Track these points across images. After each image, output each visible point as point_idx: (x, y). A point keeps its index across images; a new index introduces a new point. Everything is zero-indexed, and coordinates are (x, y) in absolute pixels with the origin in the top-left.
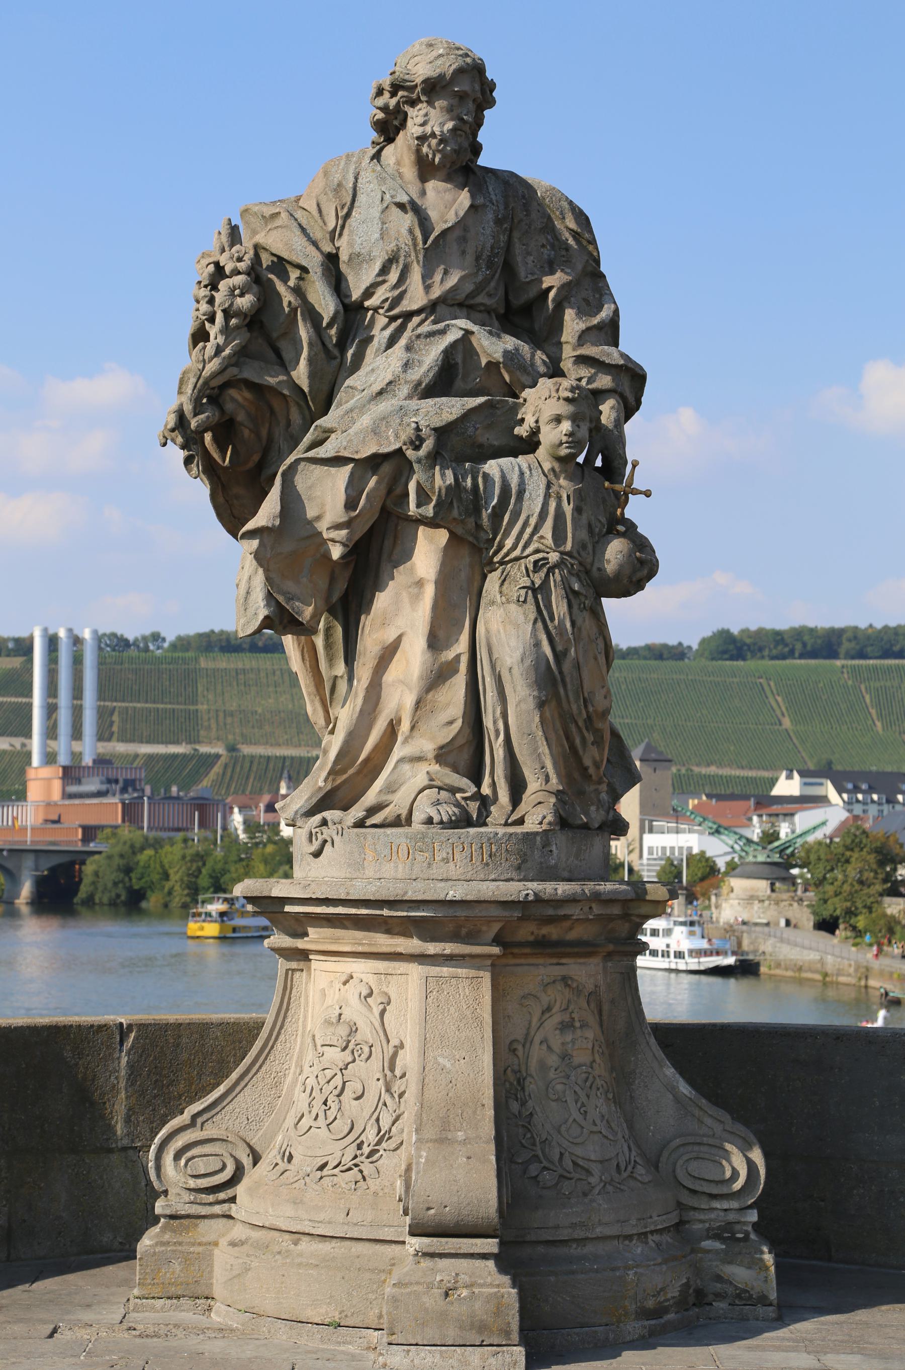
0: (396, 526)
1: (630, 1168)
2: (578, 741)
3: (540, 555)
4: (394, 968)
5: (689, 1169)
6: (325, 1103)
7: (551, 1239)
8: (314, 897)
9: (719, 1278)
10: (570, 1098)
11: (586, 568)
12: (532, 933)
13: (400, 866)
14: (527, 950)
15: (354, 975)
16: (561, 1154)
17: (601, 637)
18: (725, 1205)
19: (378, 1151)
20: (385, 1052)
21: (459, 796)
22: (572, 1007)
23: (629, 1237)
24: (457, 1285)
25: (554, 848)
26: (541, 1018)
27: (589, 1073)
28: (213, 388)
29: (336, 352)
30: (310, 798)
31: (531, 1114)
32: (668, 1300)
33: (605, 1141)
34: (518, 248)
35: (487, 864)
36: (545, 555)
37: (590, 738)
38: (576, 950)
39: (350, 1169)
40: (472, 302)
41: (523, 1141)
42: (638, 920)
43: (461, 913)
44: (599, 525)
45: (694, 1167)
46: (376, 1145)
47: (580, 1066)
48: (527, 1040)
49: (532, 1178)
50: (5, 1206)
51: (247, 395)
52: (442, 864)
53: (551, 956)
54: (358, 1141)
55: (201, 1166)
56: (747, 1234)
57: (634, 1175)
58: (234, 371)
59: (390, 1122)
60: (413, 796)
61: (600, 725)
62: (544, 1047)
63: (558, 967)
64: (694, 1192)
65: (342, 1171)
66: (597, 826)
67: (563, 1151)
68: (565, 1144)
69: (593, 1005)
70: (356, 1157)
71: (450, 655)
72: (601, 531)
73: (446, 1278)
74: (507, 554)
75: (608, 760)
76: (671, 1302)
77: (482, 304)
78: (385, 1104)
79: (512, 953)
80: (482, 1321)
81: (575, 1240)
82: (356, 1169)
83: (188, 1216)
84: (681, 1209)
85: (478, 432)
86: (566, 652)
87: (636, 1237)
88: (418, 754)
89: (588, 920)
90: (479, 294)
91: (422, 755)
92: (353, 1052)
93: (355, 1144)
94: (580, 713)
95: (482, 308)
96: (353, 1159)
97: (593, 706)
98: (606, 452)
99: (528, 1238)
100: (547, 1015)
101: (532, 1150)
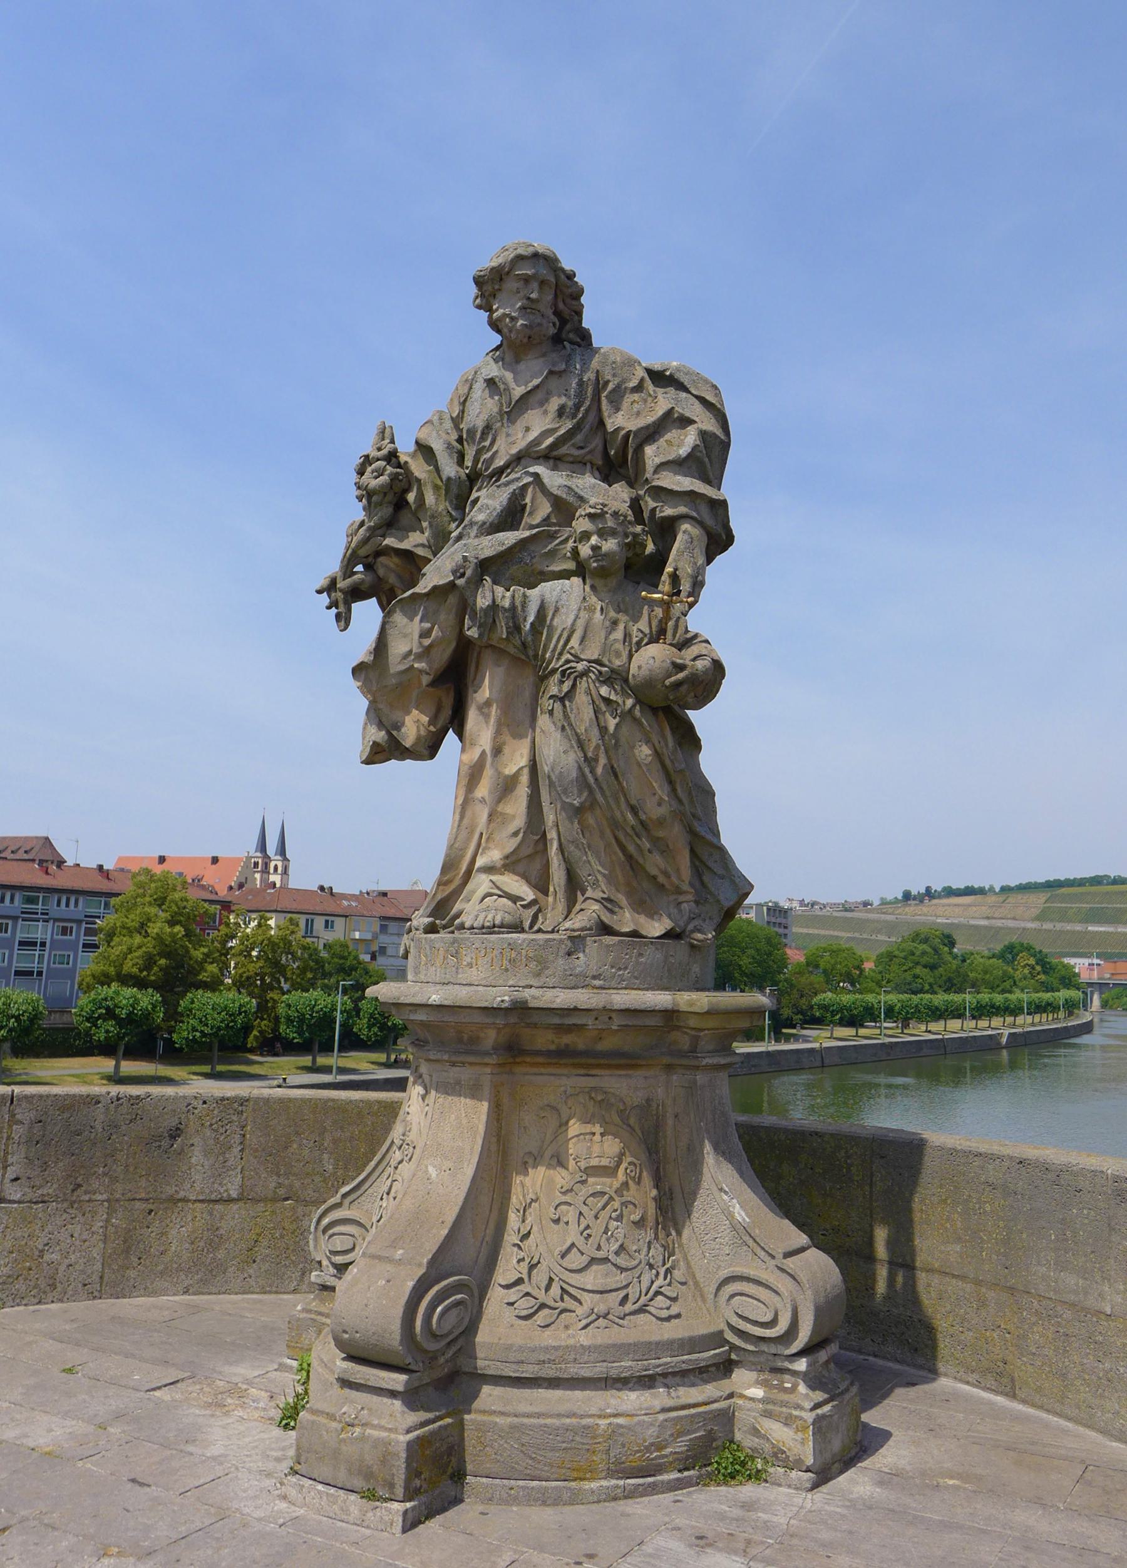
12: (553, 1042)
14: (541, 1060)
35: (507, 970)
38: (602, 1061)
40: (555, 453)
43: (449, 1018)
52: (467, 968)
53: (575, 1066)
67: (553, 1276)
68: (558, 1269)
71: (510, 770)
85: (534, 561)
86: (596, 760)
90: (564, 444)
95: (571, 459)
97: (645, 813)
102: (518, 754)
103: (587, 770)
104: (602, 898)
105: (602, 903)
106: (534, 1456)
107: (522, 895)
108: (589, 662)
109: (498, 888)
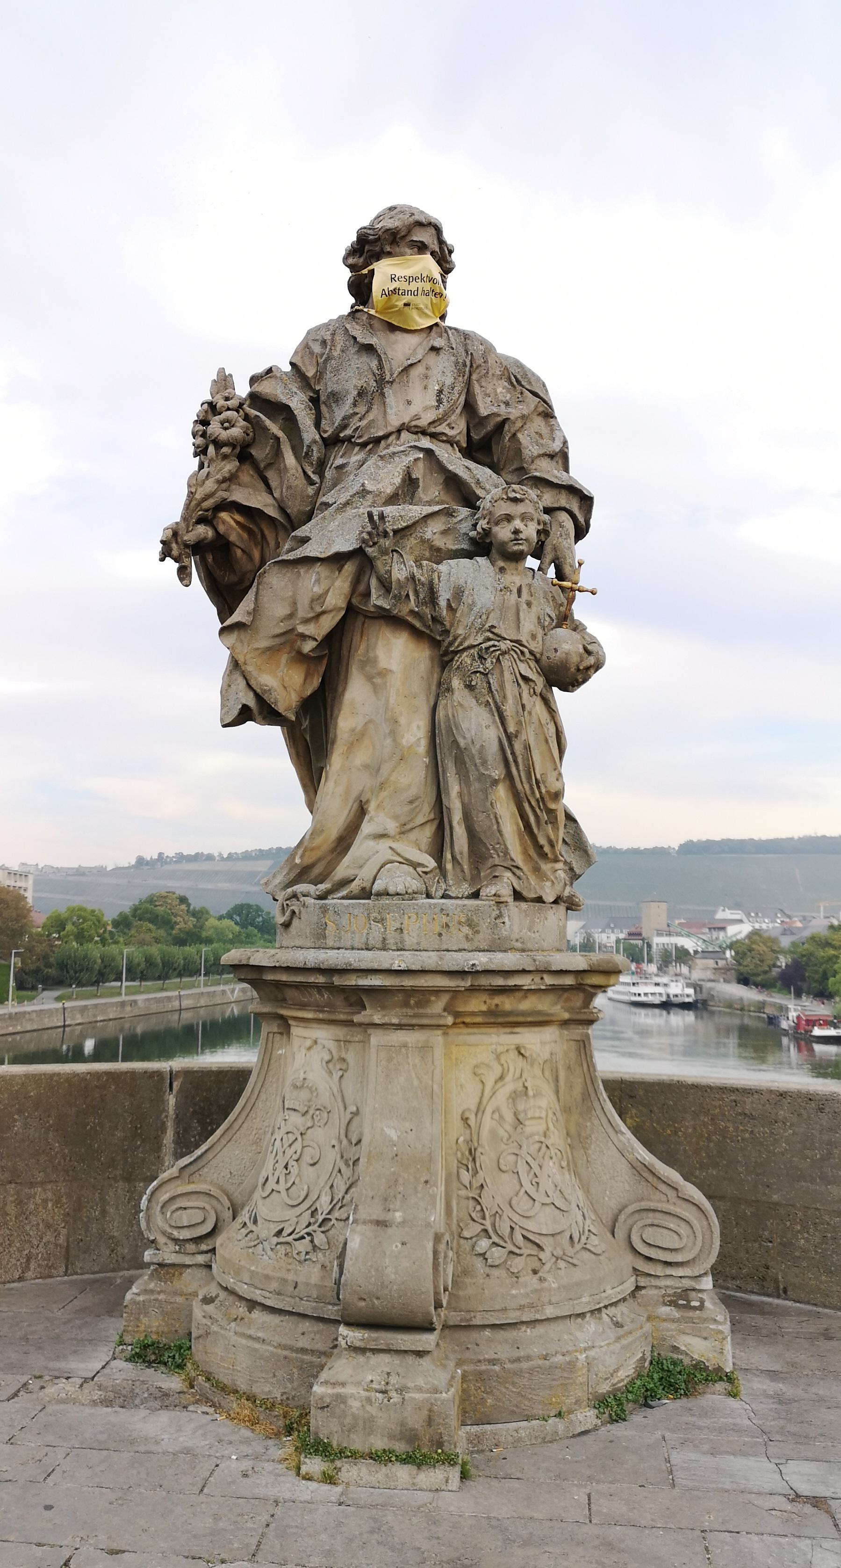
0: (363, 623)
1: (583, 1239)
2: (532, 819)
3: (491, 643)
4: (352, 1036)
5: (644, 1237)
6: (286, 1167)
7: (498, 1322)
8: (277, 965)
9: (675, 1349)
10: (522, 1168)
11: (535, 657)
13: (357, 935)
15: (319, 1041)
16: (512, 1228)
17: (553, 723)
18: (680, 1272)
19: (330, 1220)
20: (342, 1119)
21: (419, 869)
22: (525, 1076)
23: (582, 1315)
24: (390, 1387)
25: (506, 920)
26: (493, 1087)
27: (542, 1142)
28: (207, 510)
29: (315, 478)
30: (288, 874)
31: (482, 1186)
32: (623, 1380)
33: (558, 1211)
34: (477, 389)
36: (496, 643)
37: (544, 817)
39: (303, 1238)
40: (433, 430)
41: (474, 1215)
42: (592, 990)
44: (547, 619)
45: (651, 1235)
46: (329, 1213)
47: (532, 1135)
48: (480, 1110)
49: (480, 1255)
50: (64, 1227)
51: (238, 517)
54: (313, 1209)
55: (185, 1218)
56: (702, 1302)
57: (588, 1246)
58: (222, 494)
59: (343, 1188)
60: (375, 871)
61: (552, 806)
62: (496, 1116)
63: (512, 1036)
64: (649, 1259)
65: (295, 1240)
66: (552, 900)
67: (513, 1225)
68: (516, 1218)
69: (547, 1073)
70: (309, 1225)
72: (550, 624)
73: (376, 1378)
74: (461, 644)
75: (564, 840)
76: (625, 1382)
77: (443, 434)
78: (340, 1171)
79: (464, 1023)
80: (413, 1430)
81: (523, 1323)
82: (308, 1238)
83: (173, 1265)
84: (637, 1275)
85: (435, 537)
87: (588, 1315)
88: (382, 832)
89: (540, 990)
91: (384, 832)
92: (313, 1117)
93: (310, 1211)
94: (533, 792)
95: (445, 438)
96: (307, 1227)
98: (557, 562)
99: (473, 1323)
100: (500, 1084)
101: (482, 1224)
102: (414, 726)
103: (506, 744)
104: (513, 866)
105: (510, 870)
106: (530, 1396)
107: (426, 863)
108: (511, 641)
109: (399, 855)
